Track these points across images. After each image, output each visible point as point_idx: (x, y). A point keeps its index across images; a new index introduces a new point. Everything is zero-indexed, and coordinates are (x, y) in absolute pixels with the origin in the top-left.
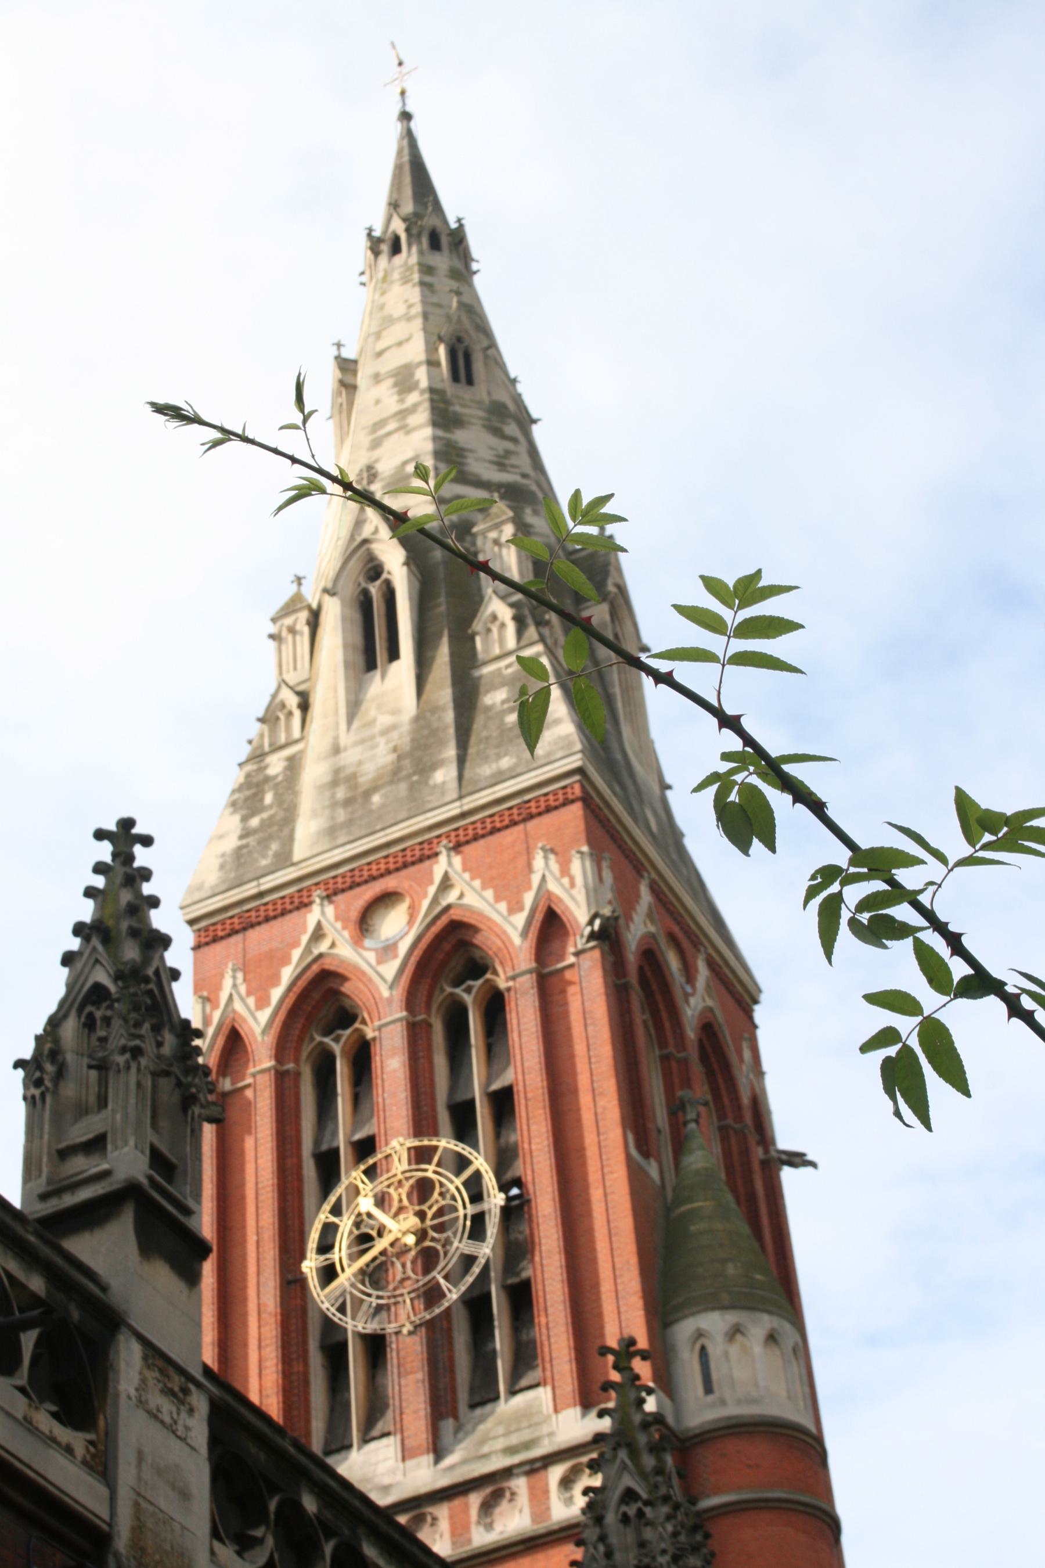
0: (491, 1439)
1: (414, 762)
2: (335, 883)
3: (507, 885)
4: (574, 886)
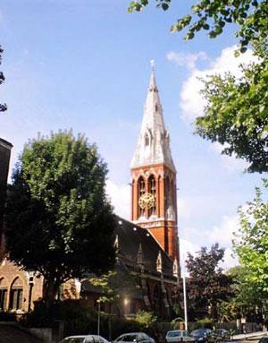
0: (151, 219)
1: (150, 158)
2: (143, 168)
3: (157, 172)
4: (161, 173)
